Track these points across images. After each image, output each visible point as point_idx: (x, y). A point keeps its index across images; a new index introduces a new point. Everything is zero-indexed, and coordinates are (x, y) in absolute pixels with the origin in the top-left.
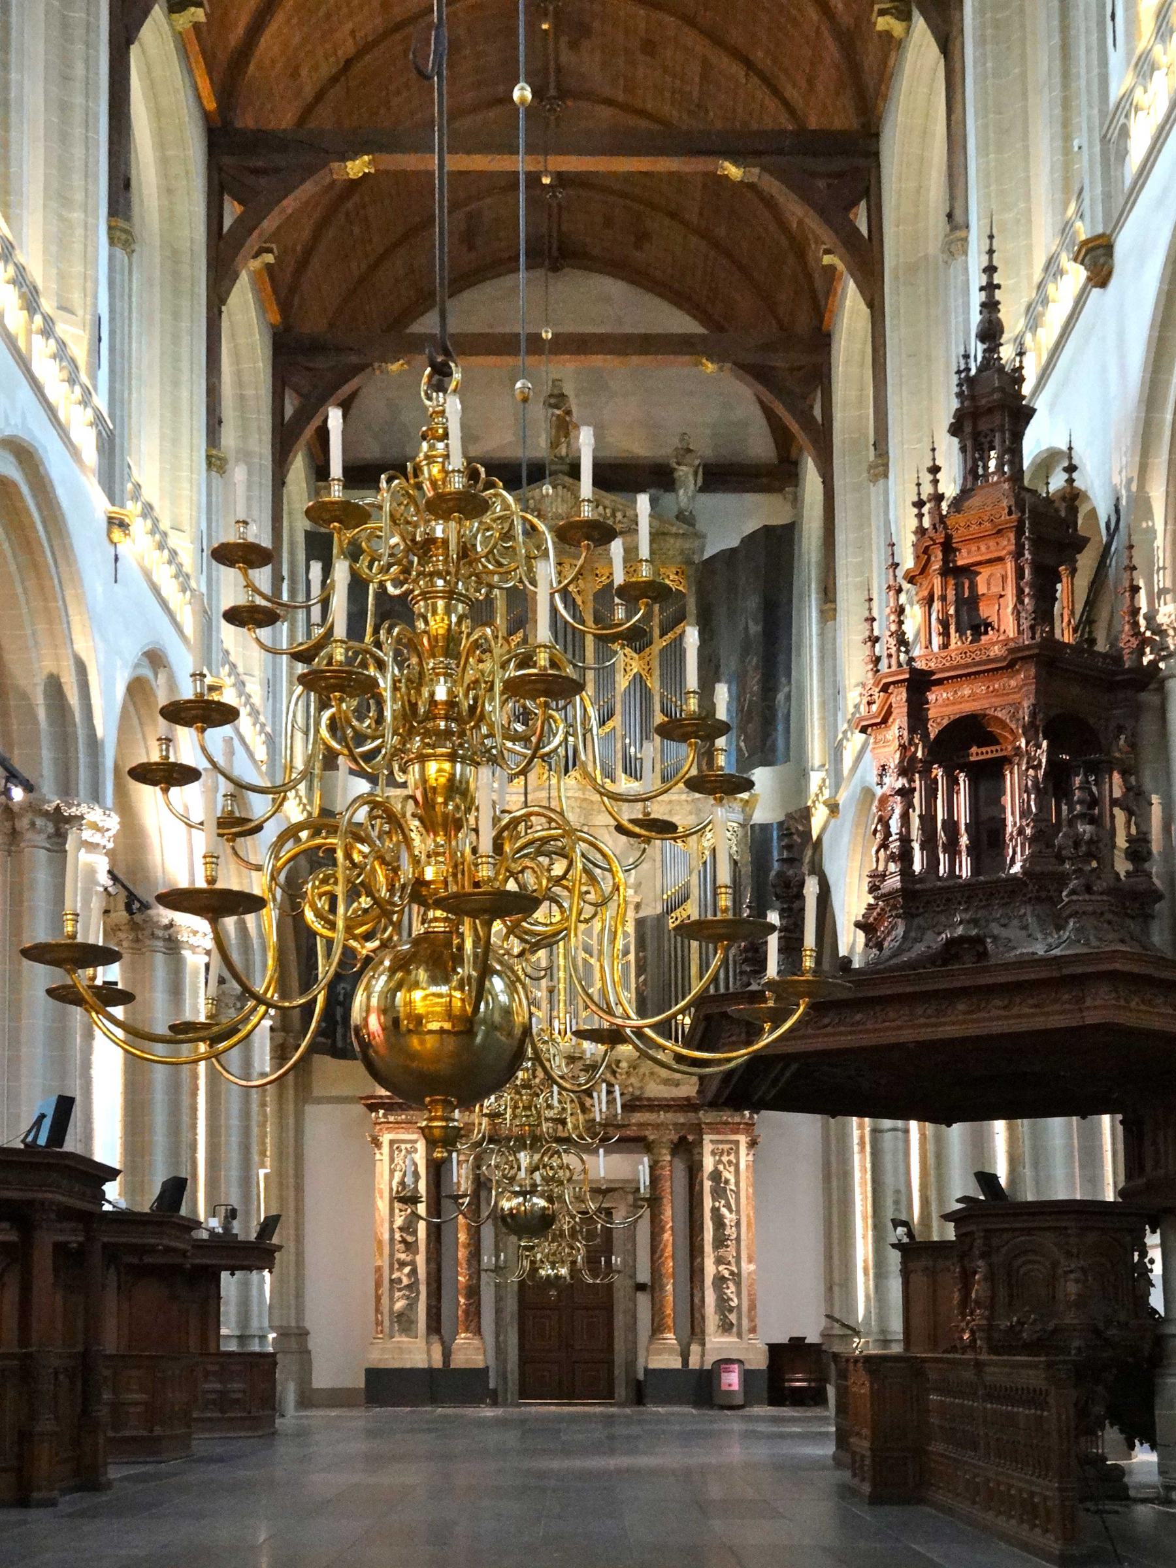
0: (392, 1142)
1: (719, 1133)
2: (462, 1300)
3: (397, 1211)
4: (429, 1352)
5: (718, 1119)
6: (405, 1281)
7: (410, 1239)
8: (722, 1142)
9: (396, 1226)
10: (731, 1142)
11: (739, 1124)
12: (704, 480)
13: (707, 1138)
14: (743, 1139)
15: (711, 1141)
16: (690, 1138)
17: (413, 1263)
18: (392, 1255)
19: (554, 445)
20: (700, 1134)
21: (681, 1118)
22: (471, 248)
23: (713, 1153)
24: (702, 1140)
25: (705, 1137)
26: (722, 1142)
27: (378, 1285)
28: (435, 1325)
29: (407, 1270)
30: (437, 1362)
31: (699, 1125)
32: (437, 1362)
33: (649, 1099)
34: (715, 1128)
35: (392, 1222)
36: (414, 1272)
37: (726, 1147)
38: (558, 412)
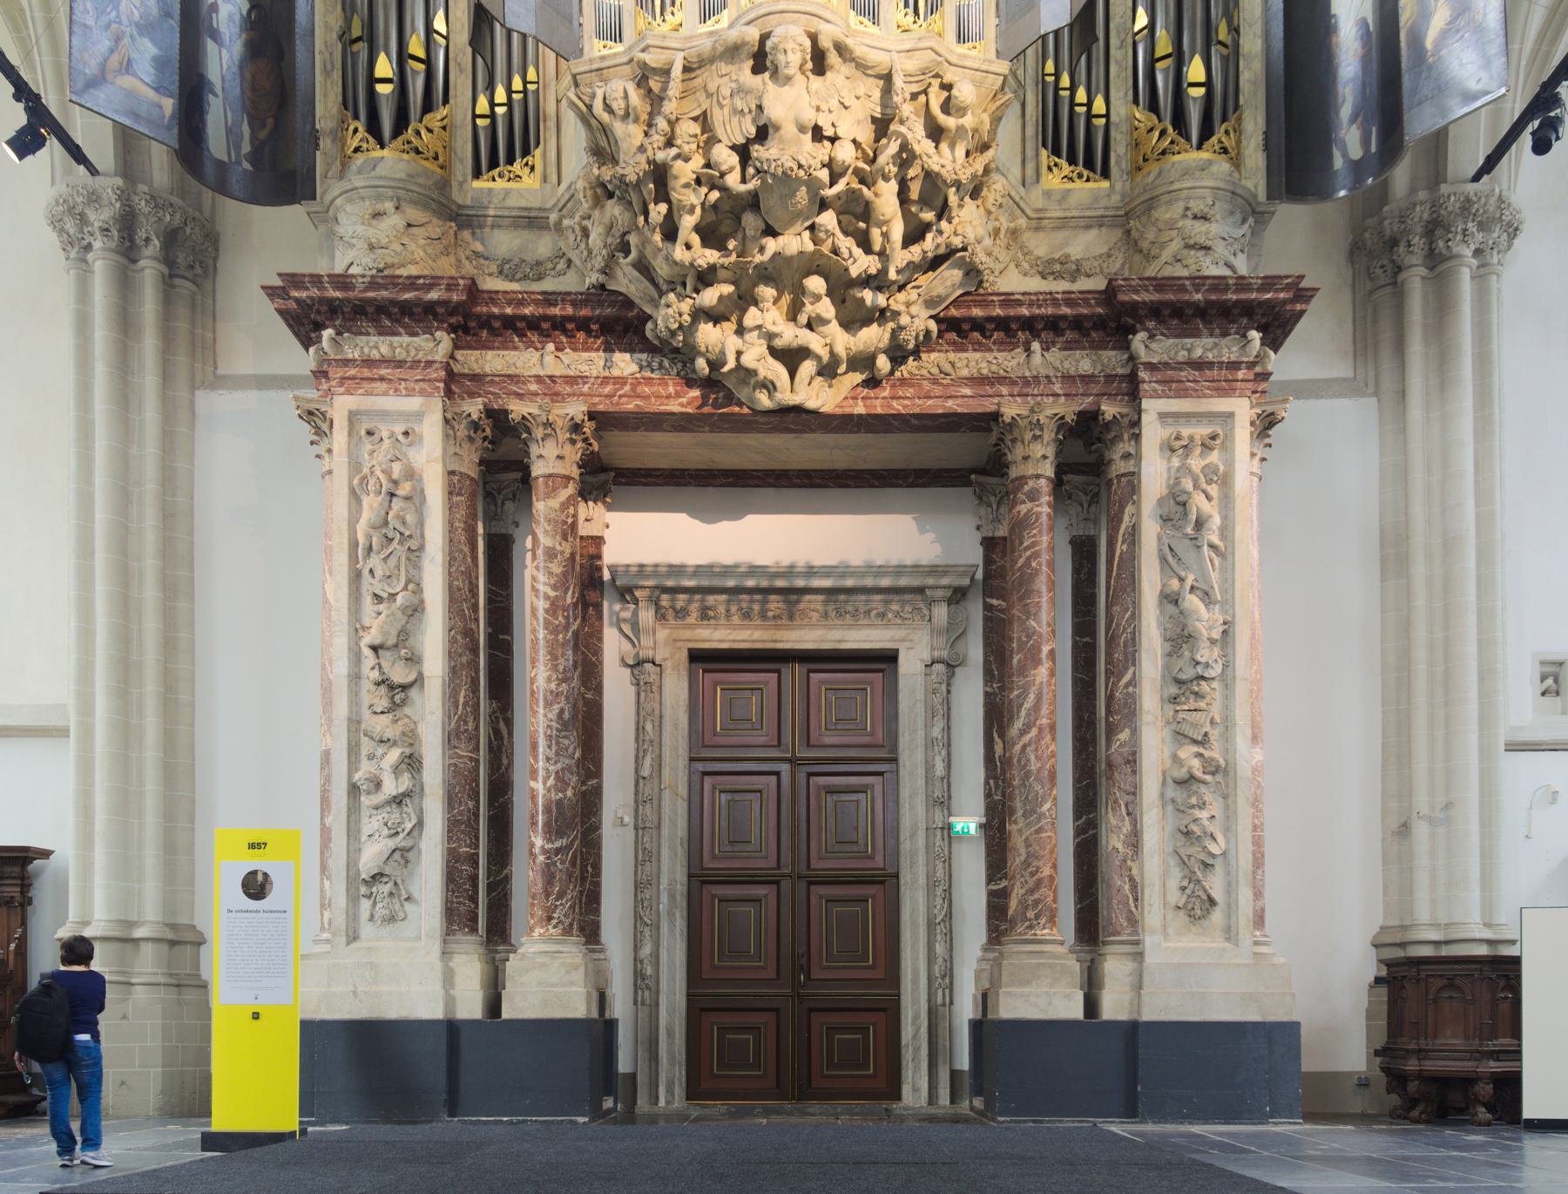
0: (353, 417)
1: (1183, 394)
5: (1182, 356)
7: (400, 675)
8: (1188, 417)
10: (1211, 416)
11: (1234, 366)
13: (1151, 407)
14: (1243, 409)
15: (1163, 416)
16: (1109, 410)
18: (354, 723)
20: (1133, 393)
21: (1083, 363)
23: (1169, 448)
24: (1139, 412)
25: (1146, 404)
26: (1188, 417)
29: (394, 755)
30: (471, 1007)
31: (1132, 380)
32: (471, 1007)
33: (1008, 300)
34: (1173, 378)
36: (412, 763)
37: (1201, 431)
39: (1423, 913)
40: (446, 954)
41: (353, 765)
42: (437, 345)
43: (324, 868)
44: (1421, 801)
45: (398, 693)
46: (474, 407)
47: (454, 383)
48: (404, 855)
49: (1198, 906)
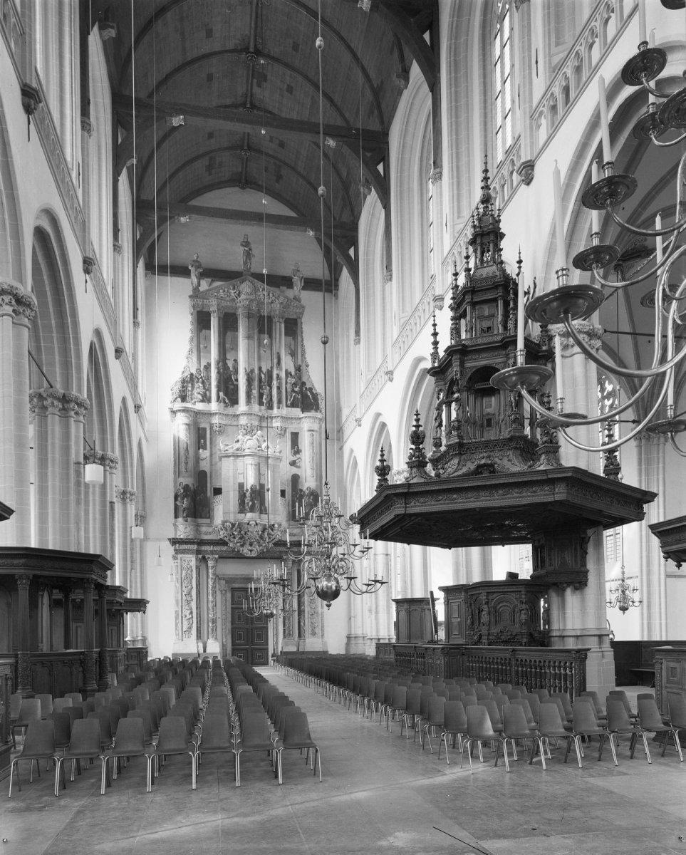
2: (210, 624)
3: (184, 588)
4: (198, 646)
6: (188, 617)
7: (189, 599)
9: (184, 594)
12: (305, 282)
17: (191, 609)
19: (245, 263)
22: (210, 174)
27: (177, 618)
28: (199, 636)
29: (189, 611)
35: (182, 591)
36: (191, 613)
38: (246, 249)
39: (353, 632)
40: (197, 643)
41: (182, 613)
42: (194, 547)
43: (176, 629)
44: (352, 615)
45: (189, 602)
46: (200, 556)
47: (198, 552)
48: (190, 628)
49: (314, 634)
